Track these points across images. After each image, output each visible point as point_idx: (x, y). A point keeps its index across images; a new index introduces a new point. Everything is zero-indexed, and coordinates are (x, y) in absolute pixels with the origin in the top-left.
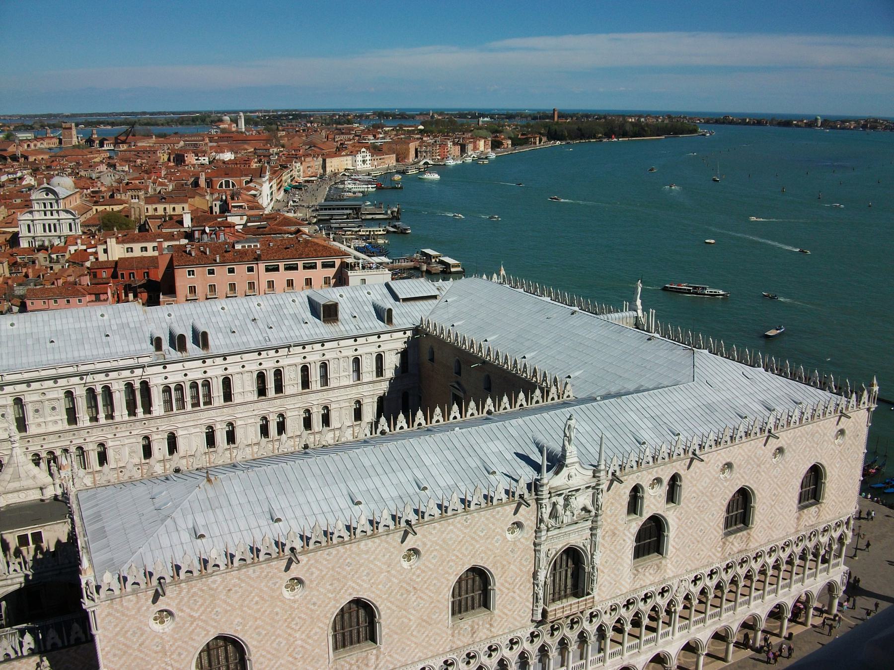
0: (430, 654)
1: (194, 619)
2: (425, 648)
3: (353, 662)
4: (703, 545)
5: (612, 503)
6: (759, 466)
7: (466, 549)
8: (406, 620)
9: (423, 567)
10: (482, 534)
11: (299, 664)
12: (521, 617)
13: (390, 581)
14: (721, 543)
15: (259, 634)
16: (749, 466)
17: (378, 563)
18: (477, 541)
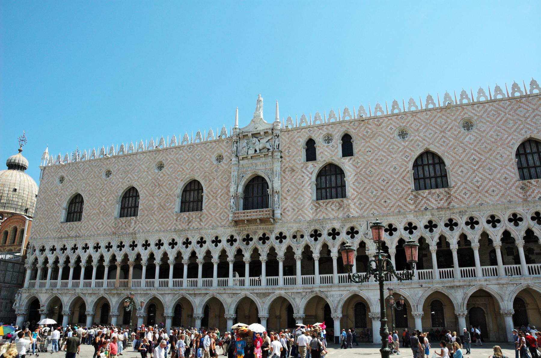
0: (163, 229)
1: (70, 181)
2: (160, 224)
3: (124, 222)
5: (289, 147)
7: (189, 165)
8: (152, 203)
9: (164, 173)
10: (198, 158)
11: (101, 215)
12: (221, 219)
13: (147, 177)
15: (89, 194)
16: (430, 131)
17: (144, 167)
18: (195, 161)
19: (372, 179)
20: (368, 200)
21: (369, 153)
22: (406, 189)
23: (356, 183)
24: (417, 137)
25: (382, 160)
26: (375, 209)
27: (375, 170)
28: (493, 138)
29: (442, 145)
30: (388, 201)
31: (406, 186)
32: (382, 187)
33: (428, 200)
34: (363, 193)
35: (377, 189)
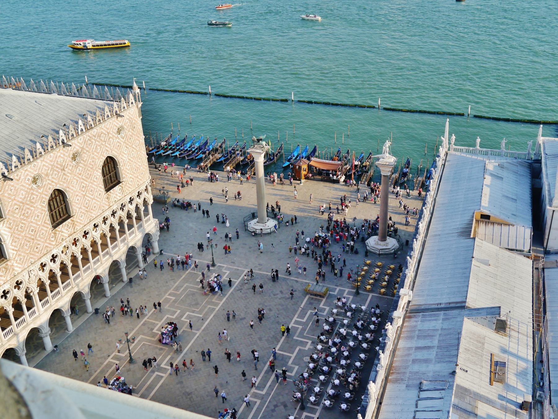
4: (38, 240)
6: (64, 170)
14: (52, 234)
16: (55, 172)
19: (24, 233)
20: (25, 253)
21: (17, 211)
22: (48, 230)
23: (13, 244)
24: (48, 181)
25: (27, 213)
26: (32, 258)
27: (24, 224)
28: (91, 164)
29: (64, 182)
30: (39, 246)
31: (48, 228)
32: (33, 237)
33: (62, 232)
34: (21, 249)
35: (30, 240)
